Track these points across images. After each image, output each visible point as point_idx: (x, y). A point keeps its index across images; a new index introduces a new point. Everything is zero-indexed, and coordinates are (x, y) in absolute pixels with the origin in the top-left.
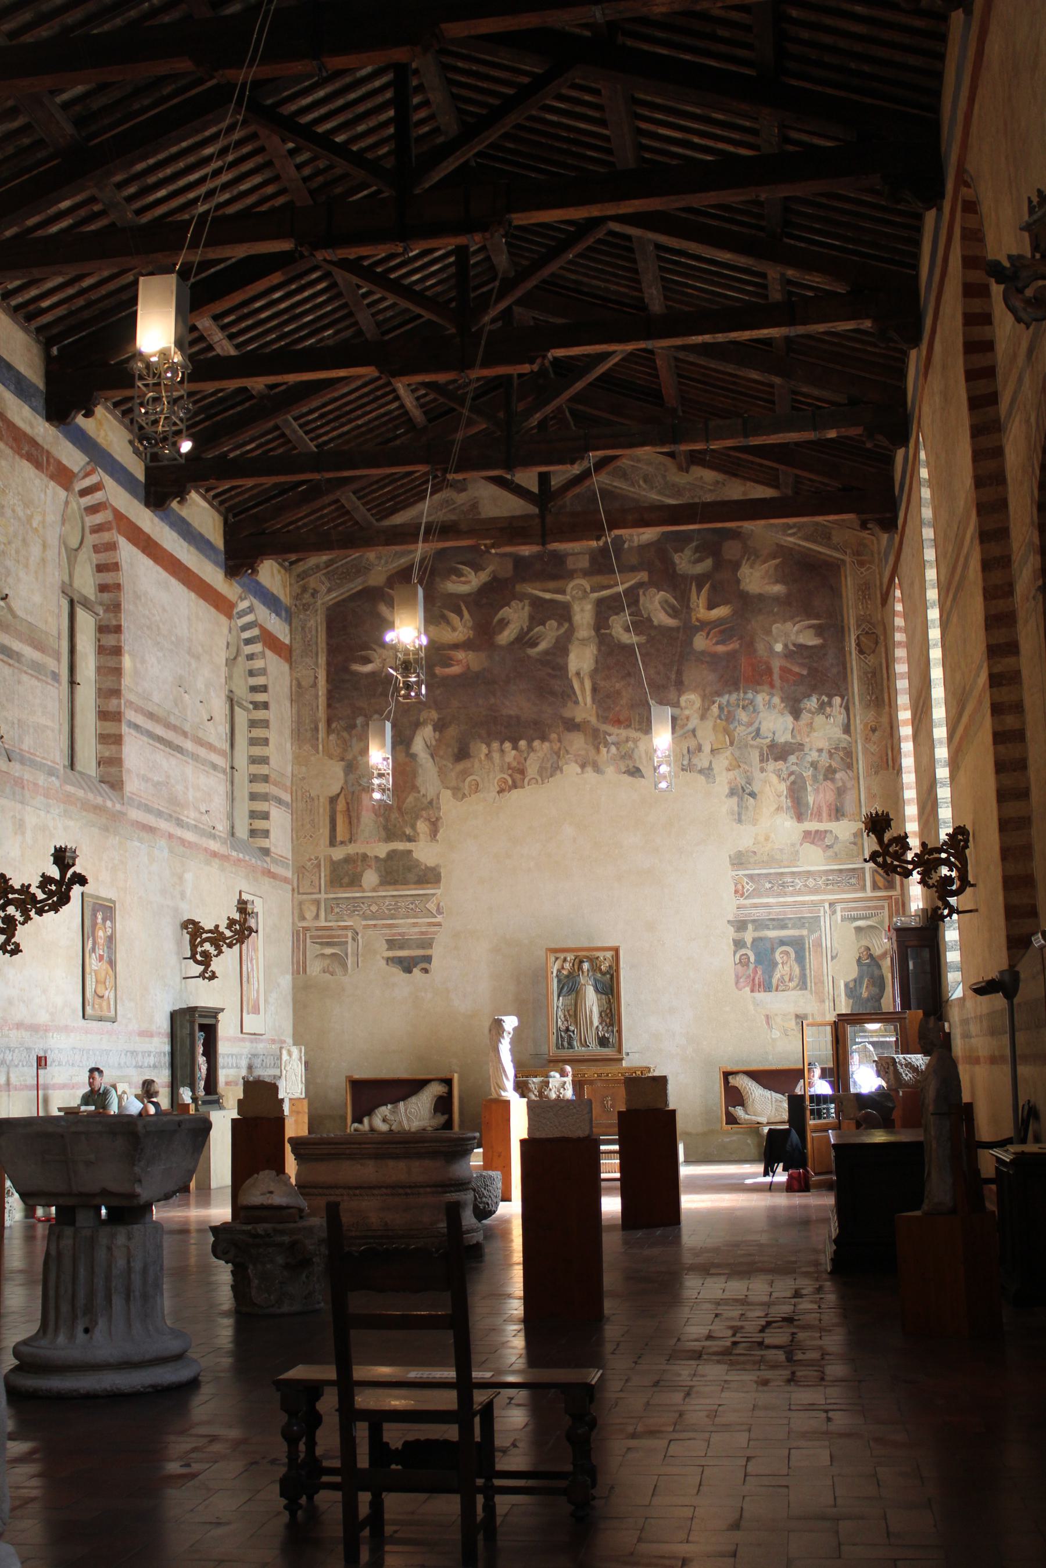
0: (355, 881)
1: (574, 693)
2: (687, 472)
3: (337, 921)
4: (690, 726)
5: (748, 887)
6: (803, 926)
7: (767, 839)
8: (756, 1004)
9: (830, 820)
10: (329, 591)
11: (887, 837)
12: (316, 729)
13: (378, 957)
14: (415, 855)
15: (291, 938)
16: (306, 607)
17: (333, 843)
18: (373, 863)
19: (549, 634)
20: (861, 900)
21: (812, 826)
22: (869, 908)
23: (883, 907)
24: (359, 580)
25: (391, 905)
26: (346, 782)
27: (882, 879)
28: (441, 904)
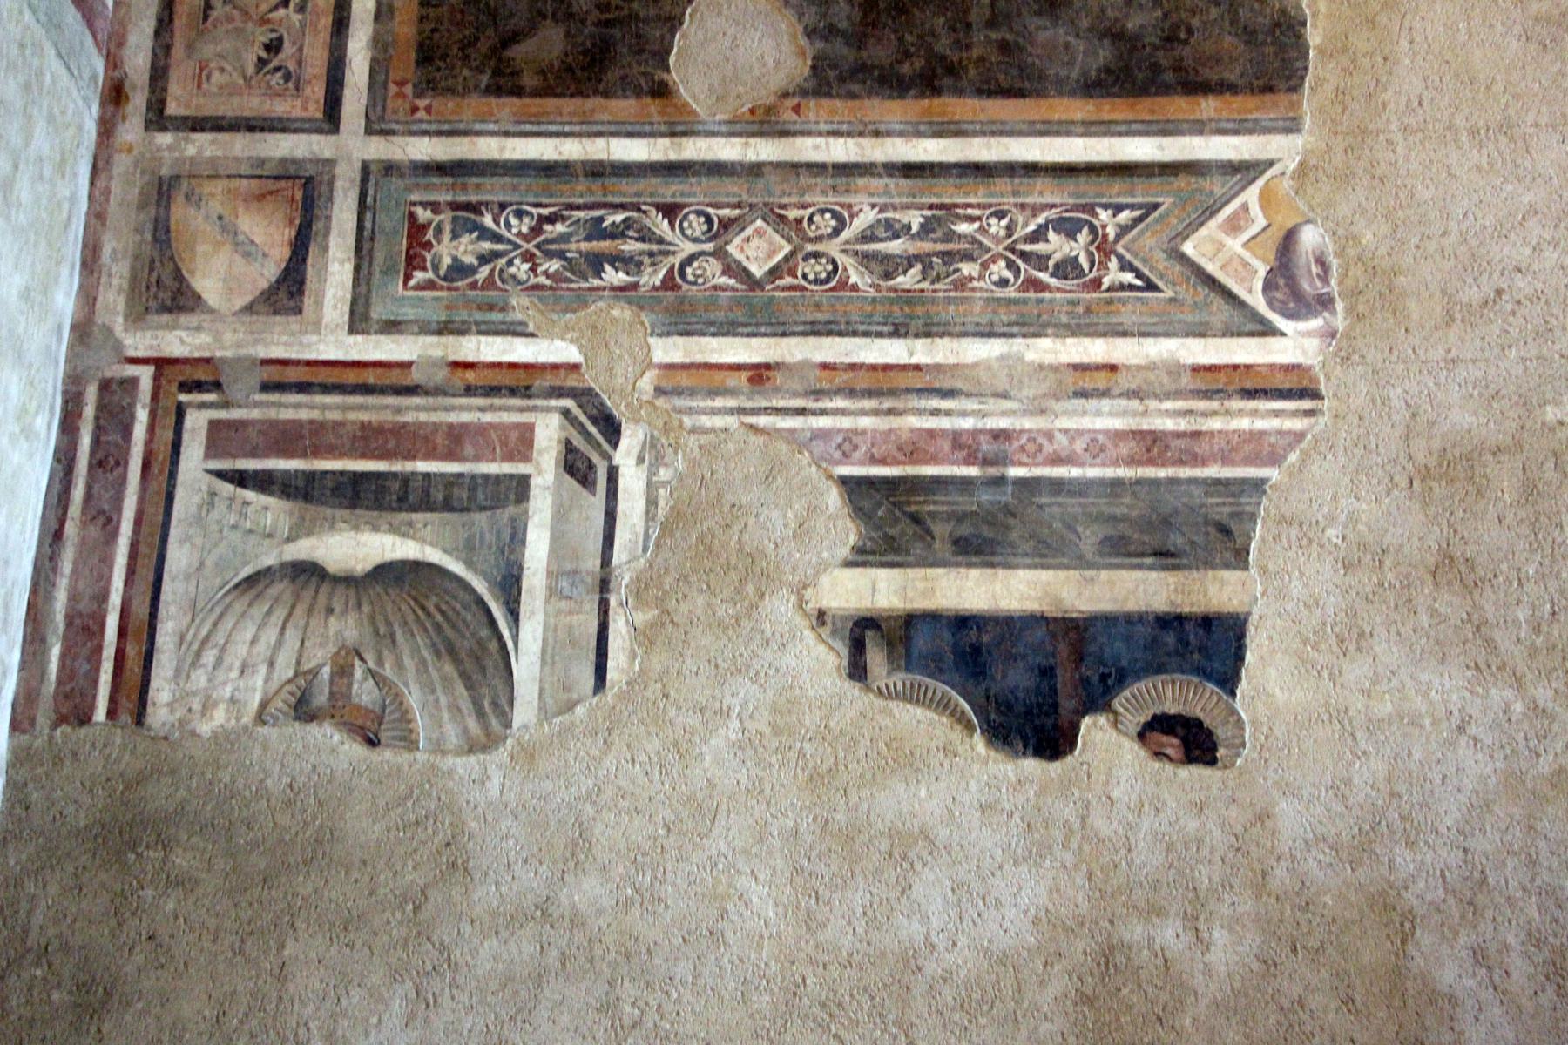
3: (444, 329)
13: (780, 608)
15: (47, 427)
25: (895, 231)
28: (1310, 238)
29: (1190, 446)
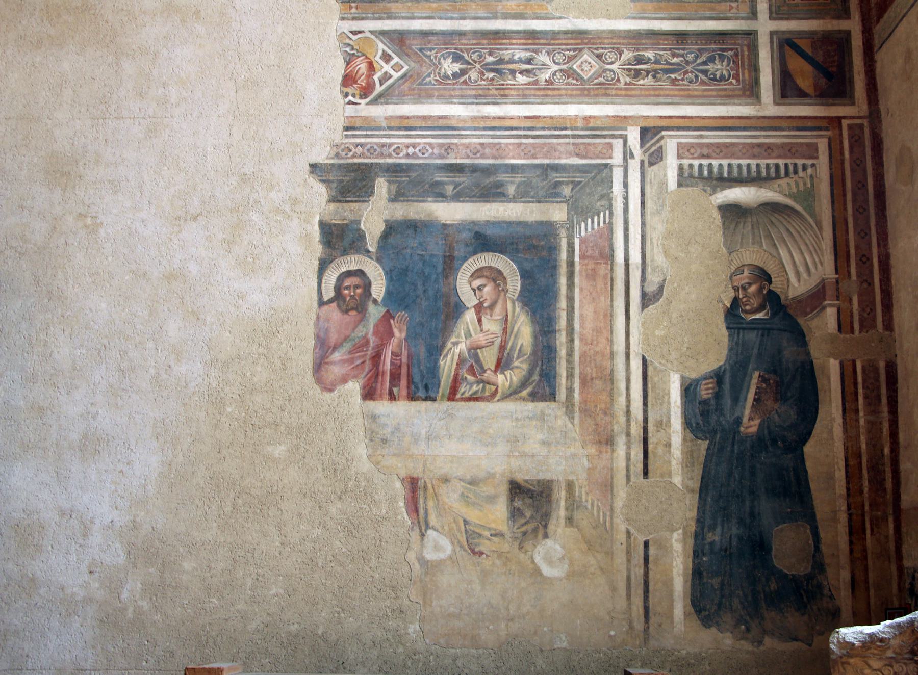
5: (387, 68)
6: (552, 194)
22: (767, 150)
23: (811, 151)
27: (808, 68)
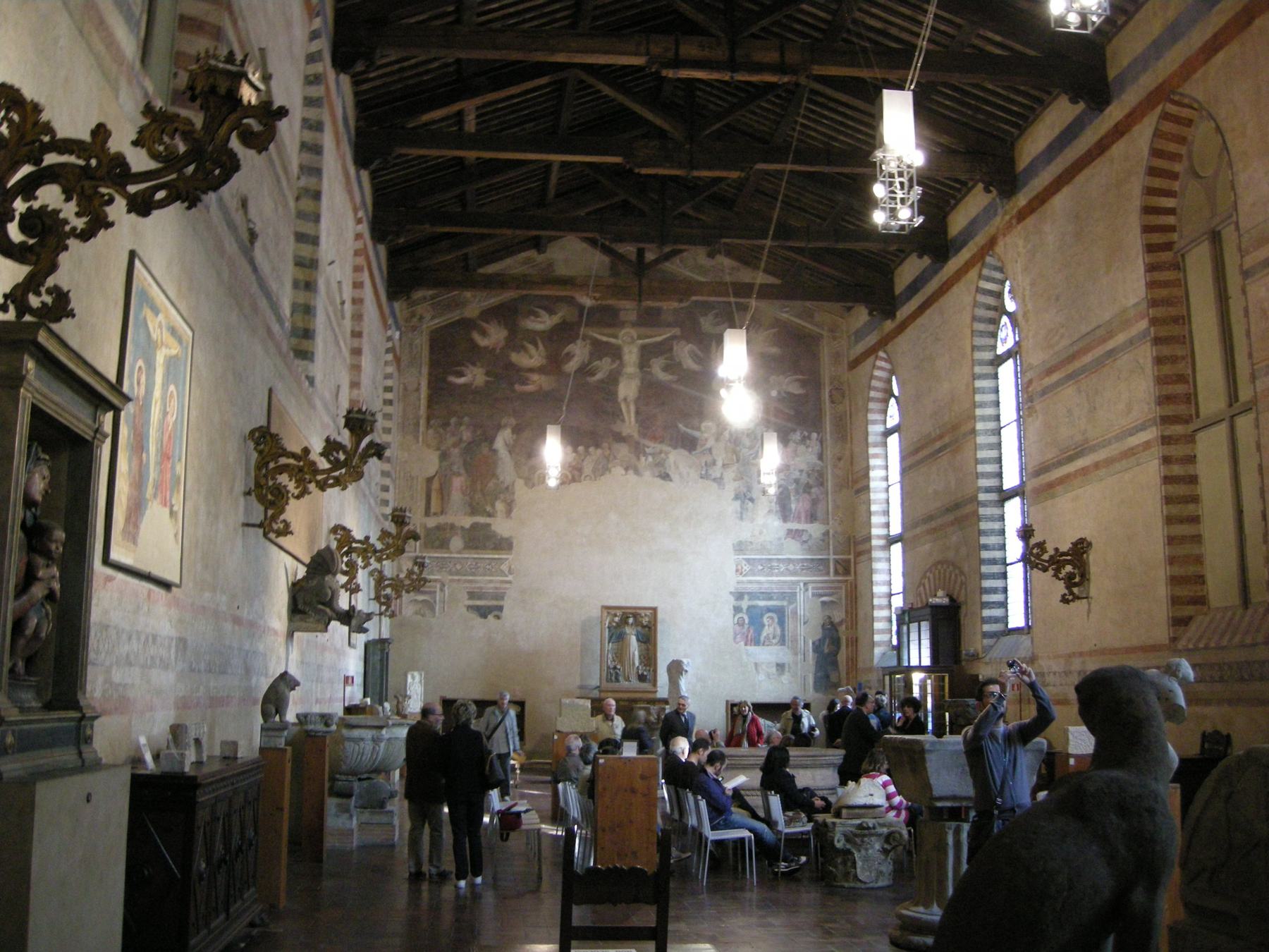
0: (444, 545)
1: (622, 414)
2: (713, 258)
4: (708, 446)
6: (784, 599)
7: (761, 533)
8: (748, 655)
9: (807, 522)
10: (433, 318)
11: (1033, 541)
12: (417, 424)
14: (493, 528)
16: (414, 329)
17: (427, 512)
18: (459, 532)
19: (604, 366)
20: (826, 582)
21: (794, 526)
22: (831, 588)
23: (841, 588)
24: (458, 312)
26: (440, 467)
29: (500, 588)
